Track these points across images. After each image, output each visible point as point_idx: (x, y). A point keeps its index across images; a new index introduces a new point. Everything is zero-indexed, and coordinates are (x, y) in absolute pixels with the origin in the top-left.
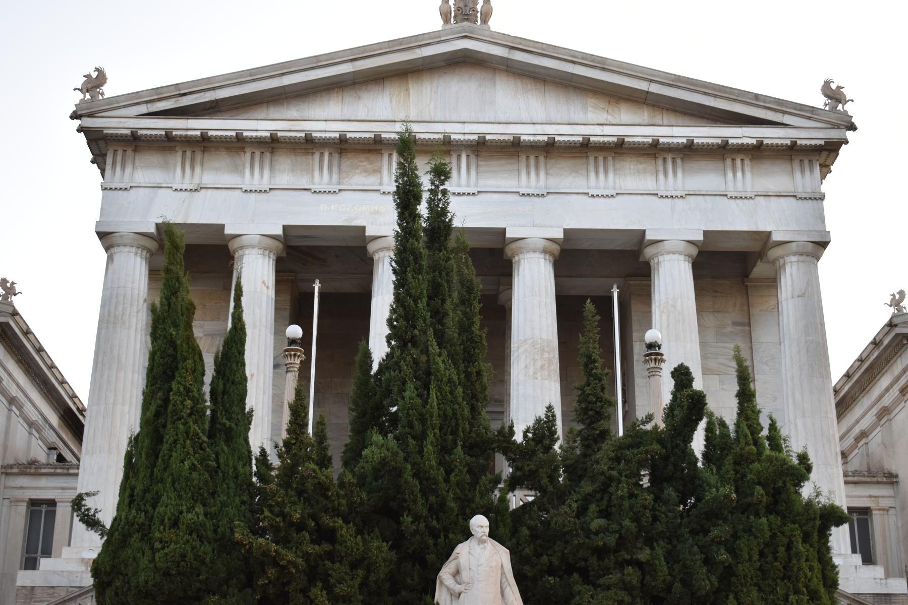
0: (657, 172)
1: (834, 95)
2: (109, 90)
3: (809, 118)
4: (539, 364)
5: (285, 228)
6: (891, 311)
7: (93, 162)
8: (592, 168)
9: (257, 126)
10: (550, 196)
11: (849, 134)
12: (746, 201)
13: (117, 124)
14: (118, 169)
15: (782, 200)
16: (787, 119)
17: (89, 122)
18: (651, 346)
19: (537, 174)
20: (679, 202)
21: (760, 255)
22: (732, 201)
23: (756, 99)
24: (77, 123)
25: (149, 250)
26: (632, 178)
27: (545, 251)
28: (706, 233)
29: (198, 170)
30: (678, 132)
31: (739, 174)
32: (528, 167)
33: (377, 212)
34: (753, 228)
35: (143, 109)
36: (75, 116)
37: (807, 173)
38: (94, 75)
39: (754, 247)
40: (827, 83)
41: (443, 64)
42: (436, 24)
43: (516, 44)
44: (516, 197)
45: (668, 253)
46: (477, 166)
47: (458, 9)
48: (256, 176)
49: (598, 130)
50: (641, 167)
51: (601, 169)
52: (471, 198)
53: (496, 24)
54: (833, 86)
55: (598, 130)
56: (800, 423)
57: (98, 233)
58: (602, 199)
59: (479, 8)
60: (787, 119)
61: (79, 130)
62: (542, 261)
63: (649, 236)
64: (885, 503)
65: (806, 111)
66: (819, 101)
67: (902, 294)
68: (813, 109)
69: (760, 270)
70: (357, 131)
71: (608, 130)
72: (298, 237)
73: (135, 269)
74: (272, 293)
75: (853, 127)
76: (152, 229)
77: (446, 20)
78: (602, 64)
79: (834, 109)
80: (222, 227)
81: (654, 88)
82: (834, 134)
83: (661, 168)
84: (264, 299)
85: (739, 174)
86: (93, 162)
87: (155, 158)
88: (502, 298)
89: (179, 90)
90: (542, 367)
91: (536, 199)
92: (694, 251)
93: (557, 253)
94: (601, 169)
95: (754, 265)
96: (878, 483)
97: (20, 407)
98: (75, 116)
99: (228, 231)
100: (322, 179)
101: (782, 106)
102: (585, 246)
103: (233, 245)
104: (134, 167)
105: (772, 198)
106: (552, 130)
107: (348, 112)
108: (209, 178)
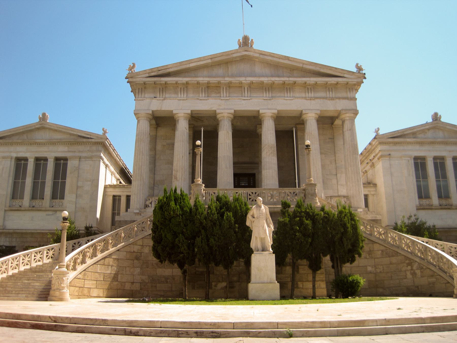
0: (305, 92)
1: (359, 68)
2: (136, 70)
4: (270, 152)
5: (191, 111)
6: (375, 134)
7: (132, 92)
8: (286, 91)
11: (364, 80)
13: (140, 80)
14: (140, 94)
16: (345, 76)
17: (131, 80)
18: (308, 146)
19: (269, 93)
20: (313, 102)
21: (337, 117)
24: (128, 80)
25: (150, 119)
28: (321, 111)
29: (164, 93)
30: (312, 80)
31: (331, 93)
32: (266, 91)
34: (335, 109)
35: (147, 75)
36: (126, 78)
37: (351, 92)
38: (132, 65)
39: (336, 115)
40: (357, 64)
42: (237, 47)
43: (262, 53)
46: (250, 91)
47: (243, 42)
48: (182, 96)
49: (287, 79)
51: (288, 91)
52: (249, 101)
53: (255, 47)
54: (359, 65)
56: (350, 169)
57: (135, 114)
59: (250, 42)
61: (128, 82)
62: (271, 120)
63: (304, 112)
64: (372, 193)
66: (355, 70)
67: (378, 129)
68: (353, 72)
69: (338, 122)
70: (213, 80)
71: (291, 79)
72: (195, 114)
73: (146, 125)
74: (188, 131)
75: (365, 78)
76: (151, 112)
77: (240, 46)
79: (359, 73)
81: (305, 66)
82: (359, 80)
83: (307, 91)
84: (186, 133)
85: (331, 93)
86: (132, 92)
88: (258, 131)
89: (158, 69)
90: (271, 153)
91: (268, 101)
92: (317, 116)
93: (275, 117)
94: (288, 91)
95: (335, 120)
96: (371, 187)
97: (109, 168)
98: (126, 78)
102: (284, 115)
103: (176, 116)
104: (145, 94)
108: (167, 96)
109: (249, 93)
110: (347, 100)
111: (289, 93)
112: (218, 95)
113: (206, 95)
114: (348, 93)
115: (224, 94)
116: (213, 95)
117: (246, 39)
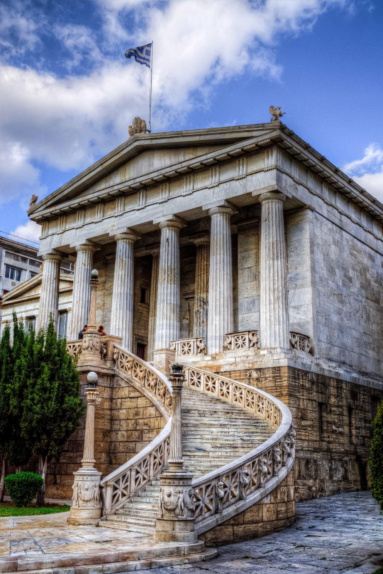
3: (263, 130)
9: (75, 202)
10: (169, 201)
12: (243, 180)
15: (258, 174)
16: (254, 134)
20: (216, 188)
22: (237, 182)
23: (239, 129)
26: (203, 182)
27: (168, 226)
33: (113, 226)
34: (245, 192)
35: (44, 206)
36: (29, 215)
37: (270, 157)
41: (136, 154)
44: (157, 205)
45: (213, 214)
49: (180, 166)
50: (204, 176)
55: (180, 166)
58: (188, 196)
60: (254, 134)
65: (260, 127)
68: (263, 125)
71: (184, 164)
78: (180, 134)
80: (69, 245)
85: (241, 167)
87: (53, 223)
99: (71, 246)
100: (98, 217)
101: (250, 128)
105: (254, 175)
106: (163, 172)
107: (107, 185)
109: (144, 199)
110: (263, 173)
111: (188, 186)
112: (113, 212)
113: (102, 214)
114: (266, 159)
115: (118, 209)
116: (109, 213)
117: (138, 121)
